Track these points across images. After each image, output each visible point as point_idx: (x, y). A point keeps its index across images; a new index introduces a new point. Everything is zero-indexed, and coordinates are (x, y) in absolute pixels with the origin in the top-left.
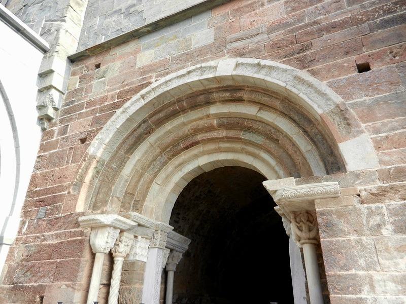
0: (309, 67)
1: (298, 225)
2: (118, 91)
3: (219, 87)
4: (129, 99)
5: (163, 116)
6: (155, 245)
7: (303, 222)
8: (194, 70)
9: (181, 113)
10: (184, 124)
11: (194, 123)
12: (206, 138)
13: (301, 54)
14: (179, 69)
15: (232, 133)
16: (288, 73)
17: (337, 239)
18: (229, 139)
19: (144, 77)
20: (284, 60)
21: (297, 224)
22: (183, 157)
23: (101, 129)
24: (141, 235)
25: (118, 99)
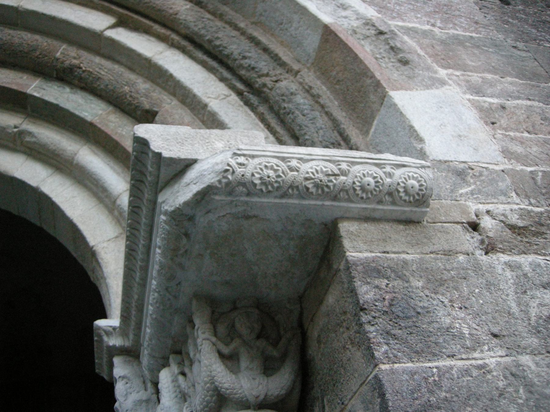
1: (226, 351)
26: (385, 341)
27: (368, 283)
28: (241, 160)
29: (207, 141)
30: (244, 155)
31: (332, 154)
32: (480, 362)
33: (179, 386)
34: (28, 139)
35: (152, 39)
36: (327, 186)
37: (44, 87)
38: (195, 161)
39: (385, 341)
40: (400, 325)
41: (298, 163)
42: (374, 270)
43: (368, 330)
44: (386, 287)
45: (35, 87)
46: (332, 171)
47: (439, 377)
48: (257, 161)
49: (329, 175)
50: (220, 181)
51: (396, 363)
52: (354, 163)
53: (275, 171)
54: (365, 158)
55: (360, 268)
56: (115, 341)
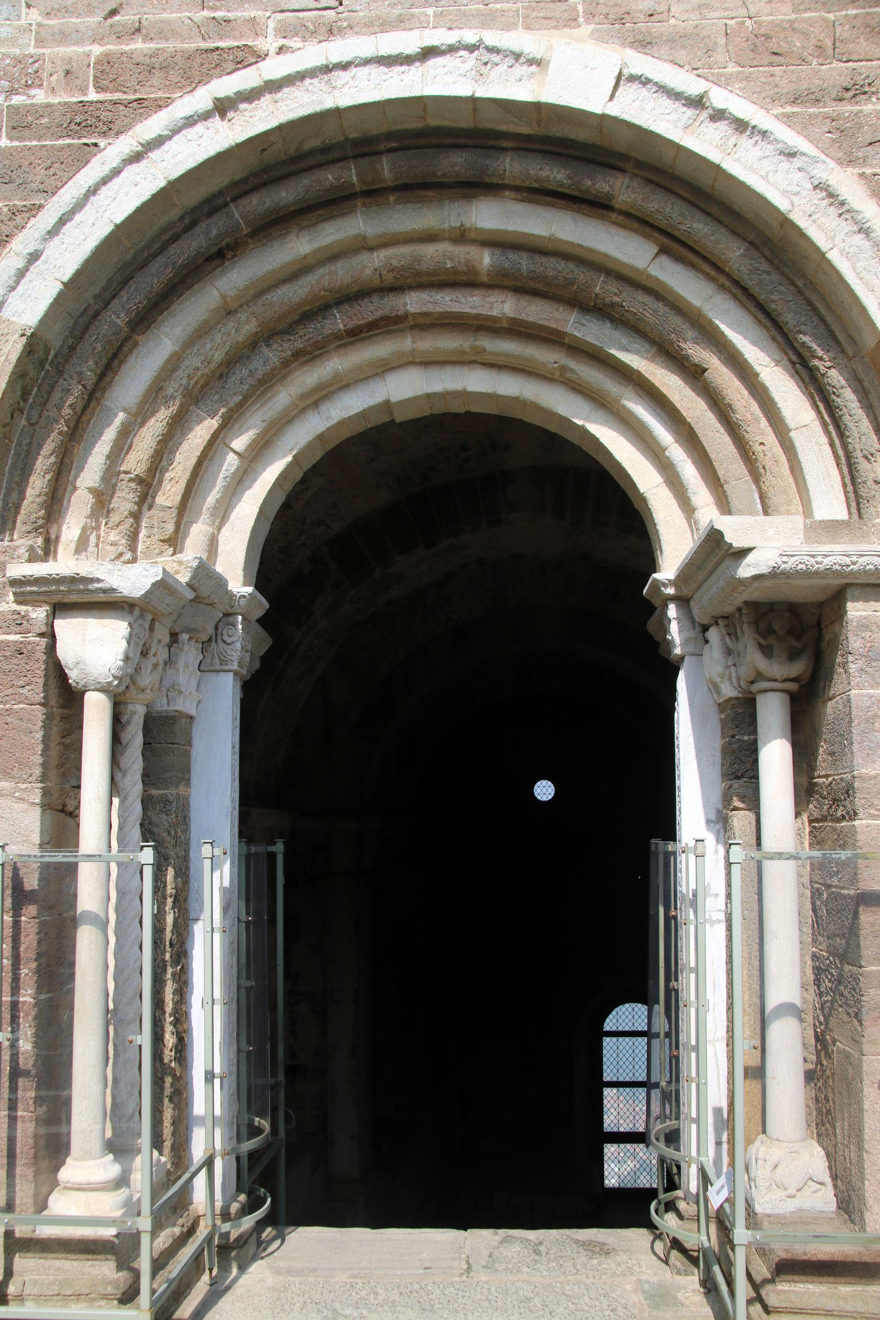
0: (865, 161)
2: (97, 50)
3: (529, 138)
4: (160, 105)
5: (291, 198)
6: (222, 662)
8: (452, 49)
9: (359, 202)
10: (364, 245)
11: (405, 250)
12: (438, 309)
13: (847, 108)
14: (385, 25)
15: (537, 312)
16: (797, 162)
18: (518, 330)
19: (219, 14)
20: (789, 109)
22: (334, 364)
23: (35, 210)
24: (187, 630)
25: (99, 89)
28: (785, 559)
33: (725, 644)
34: (568, 375)
35: (699, 275)
37: (584, 321)
42: (864, 625)
45: (574, 322)
48: (795, 558)
50: (770, 573)
52: (862, 556)
53: (807, 565)
55: (855, 624)
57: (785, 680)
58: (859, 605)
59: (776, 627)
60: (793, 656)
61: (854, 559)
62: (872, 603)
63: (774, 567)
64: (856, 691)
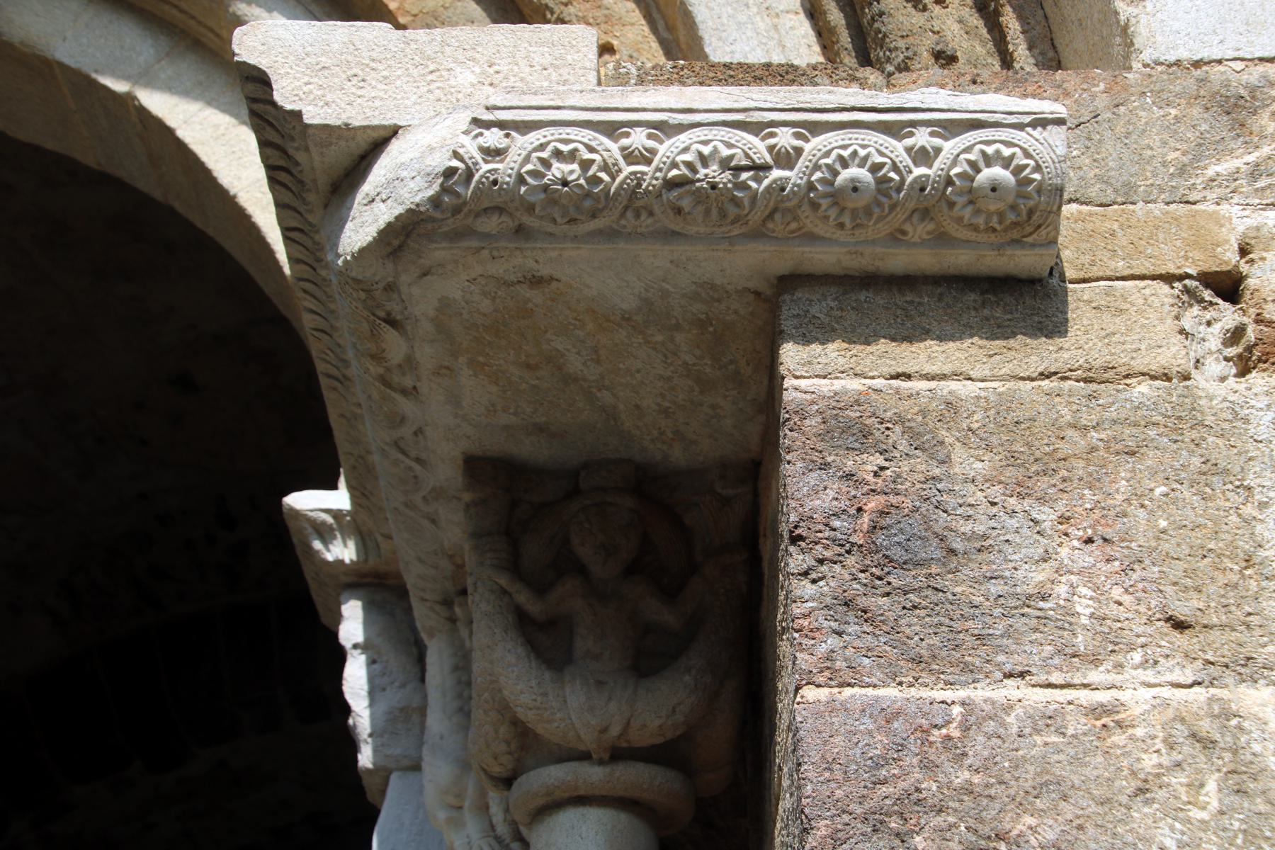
1: (534, 607)
7: (581, 570)
17: (980, 693)
21: (523, 597)
26: (834, 625)
27: (825, 466)
28: (493, 138)
29: (432, 67)
30: (501, 125)
31: (753, 104)
32: (1102, 697)
36: (735, 202)
38: (394, 131)
39: (834, 625)
40: (889, 583)
41: (650, 136)
42: (851, 427)
43: (798, 592)
44: (876, 474)
46: (747, 156)
47: (965, 728)
48: (535, 137)
49: (739, 169)
50: (435, 201)
51: (849, 685)
52: (816, 128)
53: (586, 165)
54: (853, 109)
55: (812, 423)
56: (343, 551)
57: (618, 754)
58: (833, 353)
59: (585, 551)
60: (647, 659)
61: (785, 138)
62: (883, 345)
63: (449, 172)
64: (823, 694)
